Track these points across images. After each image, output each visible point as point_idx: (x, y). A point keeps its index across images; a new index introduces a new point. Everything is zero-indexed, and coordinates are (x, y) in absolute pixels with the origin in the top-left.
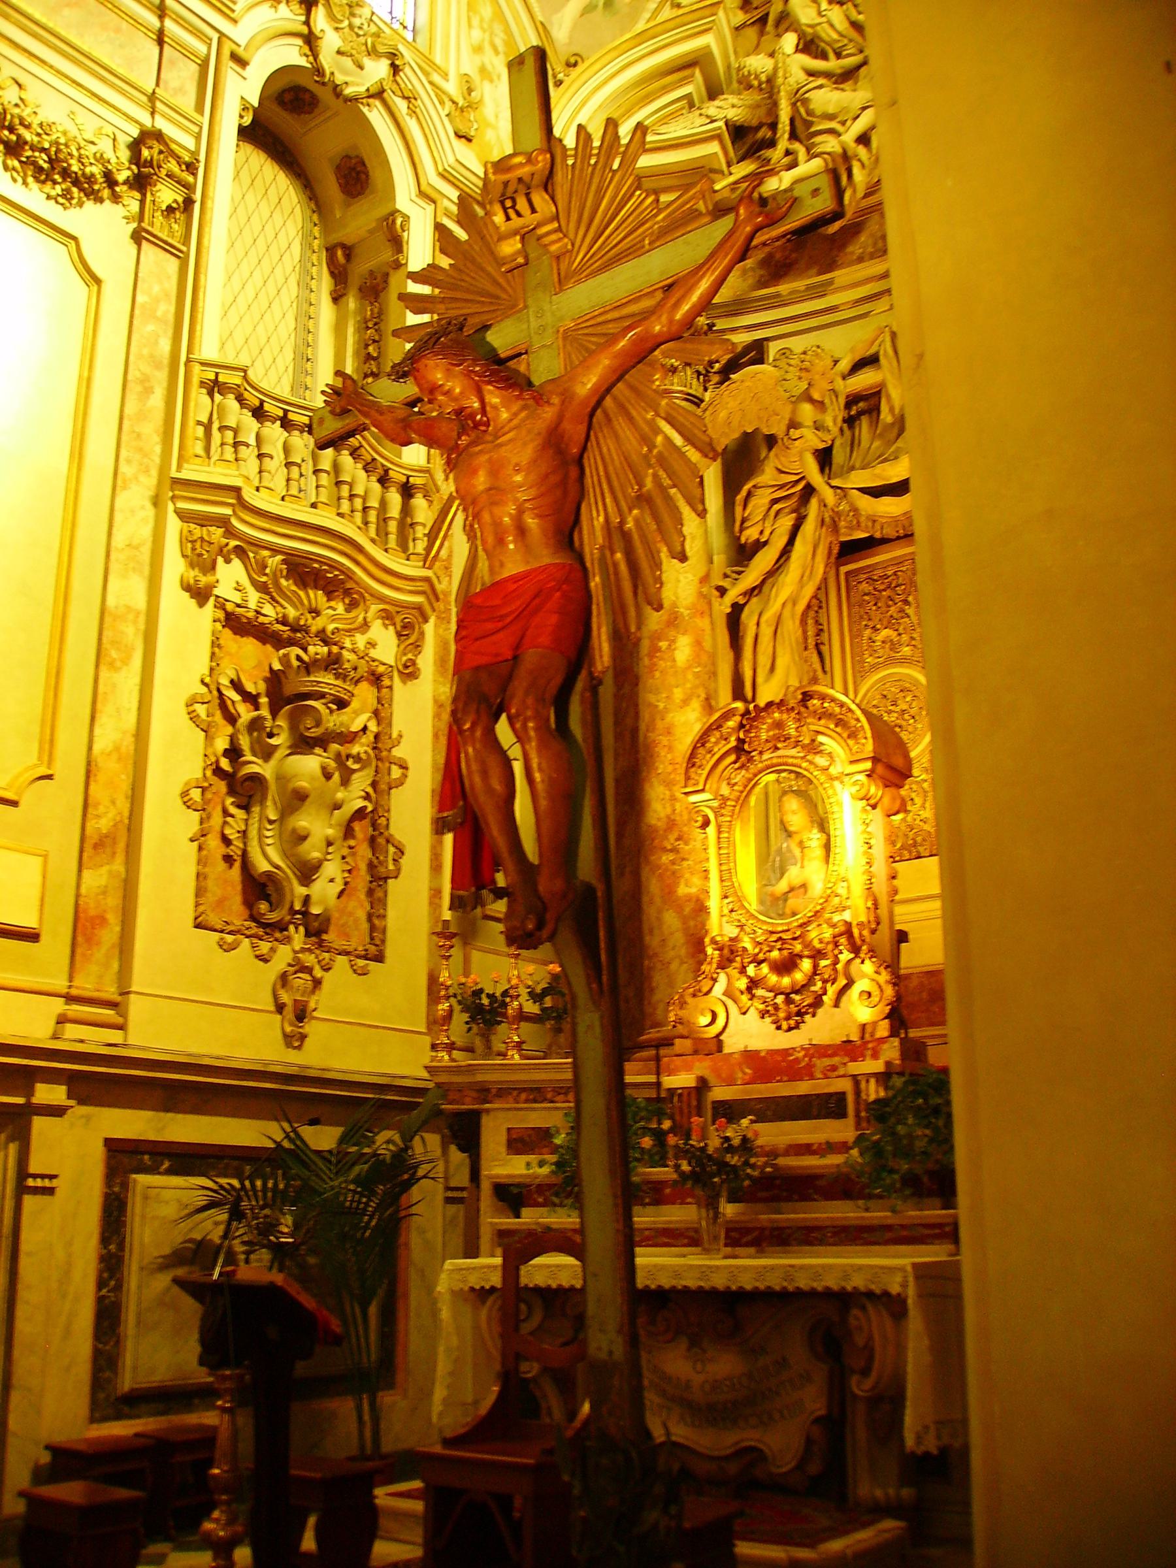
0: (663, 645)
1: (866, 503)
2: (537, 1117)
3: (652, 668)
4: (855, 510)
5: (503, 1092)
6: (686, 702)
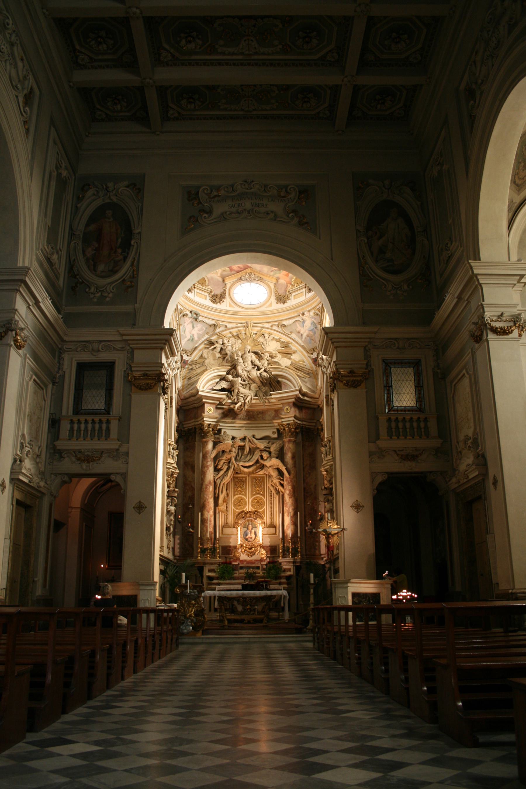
0: (208, 487)
1: (242, 468)
2: (212, 567)
3: (206, 491)
4: (240, 469)
5: (208, 563)
6: (211, 498)
